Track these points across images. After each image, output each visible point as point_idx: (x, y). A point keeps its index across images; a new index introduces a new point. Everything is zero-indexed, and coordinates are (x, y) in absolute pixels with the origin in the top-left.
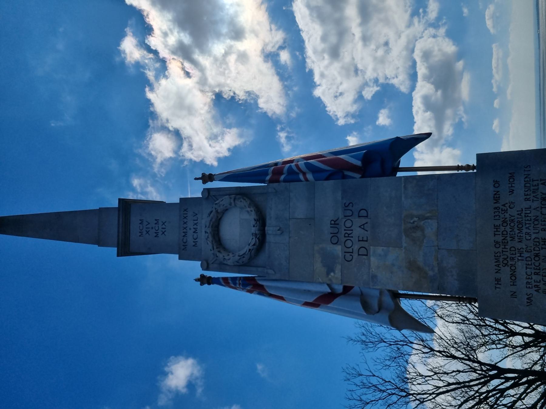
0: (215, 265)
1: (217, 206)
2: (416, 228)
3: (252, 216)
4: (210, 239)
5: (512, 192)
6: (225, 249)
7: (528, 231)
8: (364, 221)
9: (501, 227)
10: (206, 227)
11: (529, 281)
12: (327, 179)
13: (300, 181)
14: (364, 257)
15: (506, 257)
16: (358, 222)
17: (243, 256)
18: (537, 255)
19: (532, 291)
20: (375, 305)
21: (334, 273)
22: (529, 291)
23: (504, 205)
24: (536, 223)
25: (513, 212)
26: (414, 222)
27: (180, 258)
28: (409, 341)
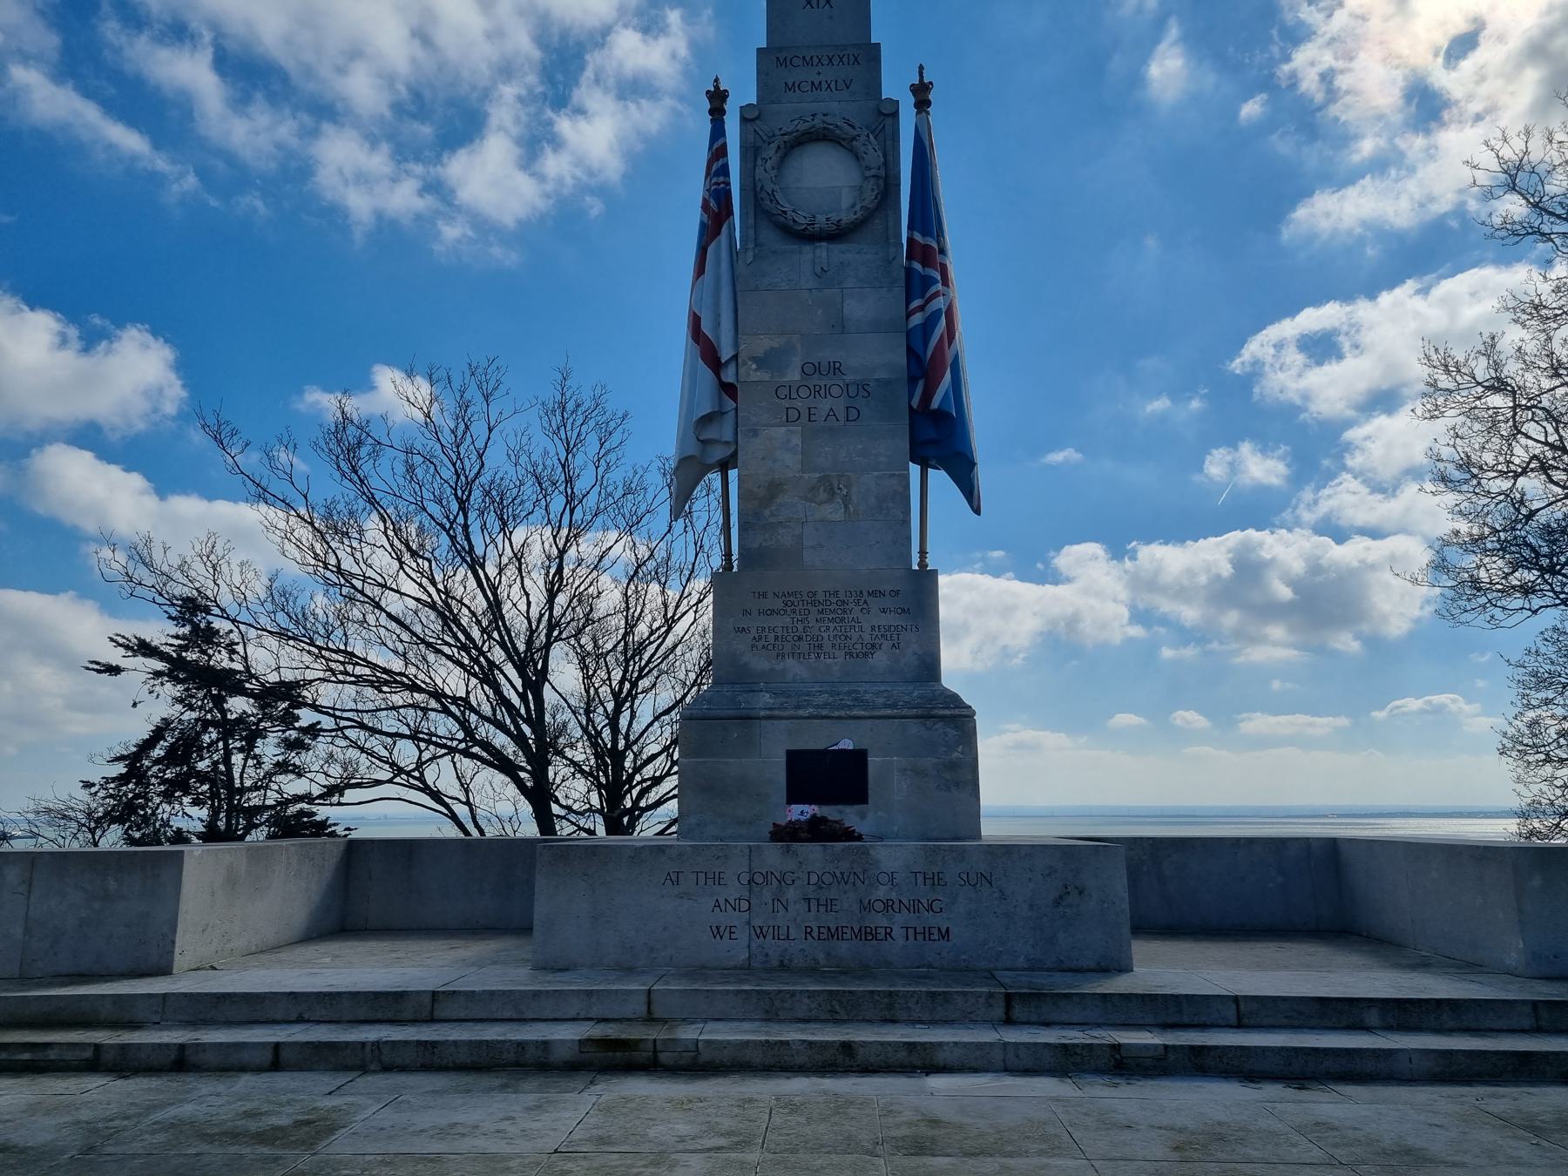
0: (751, 138)
1: (863, 138)
2: (832, 493)
3: (847, 217)
4: (803, 127)
5: (884, 611)
6: (783, 159)
7: (831, 629)
8: (842, 417)
9: (836, 599)
10: (824, 115)
11: (767, 630)
12: (910, 351)
13: (908, 303)
14: (785, 418)
15: (796, 604)
16: (840, 406)
17: (773, 199)
18: (800, 638)
19: (754, 633)
20: (709, 434)
21: (756, 370)
22: (754, 631)
23: (865, 602)
24: (843, 638)
25: (856, 613)
26: (839, 489)
27: (759, 50)
28: (575, 508)
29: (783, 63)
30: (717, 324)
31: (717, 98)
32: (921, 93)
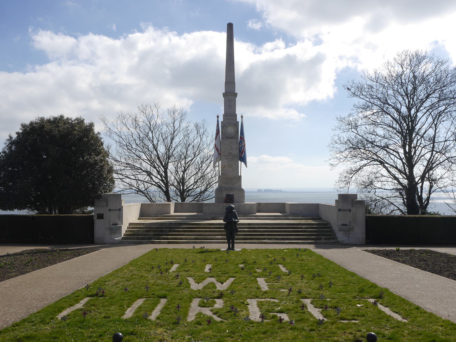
29: (226, 116)
30: (218, 146)
31: (218, 117)
32: (242, 117)
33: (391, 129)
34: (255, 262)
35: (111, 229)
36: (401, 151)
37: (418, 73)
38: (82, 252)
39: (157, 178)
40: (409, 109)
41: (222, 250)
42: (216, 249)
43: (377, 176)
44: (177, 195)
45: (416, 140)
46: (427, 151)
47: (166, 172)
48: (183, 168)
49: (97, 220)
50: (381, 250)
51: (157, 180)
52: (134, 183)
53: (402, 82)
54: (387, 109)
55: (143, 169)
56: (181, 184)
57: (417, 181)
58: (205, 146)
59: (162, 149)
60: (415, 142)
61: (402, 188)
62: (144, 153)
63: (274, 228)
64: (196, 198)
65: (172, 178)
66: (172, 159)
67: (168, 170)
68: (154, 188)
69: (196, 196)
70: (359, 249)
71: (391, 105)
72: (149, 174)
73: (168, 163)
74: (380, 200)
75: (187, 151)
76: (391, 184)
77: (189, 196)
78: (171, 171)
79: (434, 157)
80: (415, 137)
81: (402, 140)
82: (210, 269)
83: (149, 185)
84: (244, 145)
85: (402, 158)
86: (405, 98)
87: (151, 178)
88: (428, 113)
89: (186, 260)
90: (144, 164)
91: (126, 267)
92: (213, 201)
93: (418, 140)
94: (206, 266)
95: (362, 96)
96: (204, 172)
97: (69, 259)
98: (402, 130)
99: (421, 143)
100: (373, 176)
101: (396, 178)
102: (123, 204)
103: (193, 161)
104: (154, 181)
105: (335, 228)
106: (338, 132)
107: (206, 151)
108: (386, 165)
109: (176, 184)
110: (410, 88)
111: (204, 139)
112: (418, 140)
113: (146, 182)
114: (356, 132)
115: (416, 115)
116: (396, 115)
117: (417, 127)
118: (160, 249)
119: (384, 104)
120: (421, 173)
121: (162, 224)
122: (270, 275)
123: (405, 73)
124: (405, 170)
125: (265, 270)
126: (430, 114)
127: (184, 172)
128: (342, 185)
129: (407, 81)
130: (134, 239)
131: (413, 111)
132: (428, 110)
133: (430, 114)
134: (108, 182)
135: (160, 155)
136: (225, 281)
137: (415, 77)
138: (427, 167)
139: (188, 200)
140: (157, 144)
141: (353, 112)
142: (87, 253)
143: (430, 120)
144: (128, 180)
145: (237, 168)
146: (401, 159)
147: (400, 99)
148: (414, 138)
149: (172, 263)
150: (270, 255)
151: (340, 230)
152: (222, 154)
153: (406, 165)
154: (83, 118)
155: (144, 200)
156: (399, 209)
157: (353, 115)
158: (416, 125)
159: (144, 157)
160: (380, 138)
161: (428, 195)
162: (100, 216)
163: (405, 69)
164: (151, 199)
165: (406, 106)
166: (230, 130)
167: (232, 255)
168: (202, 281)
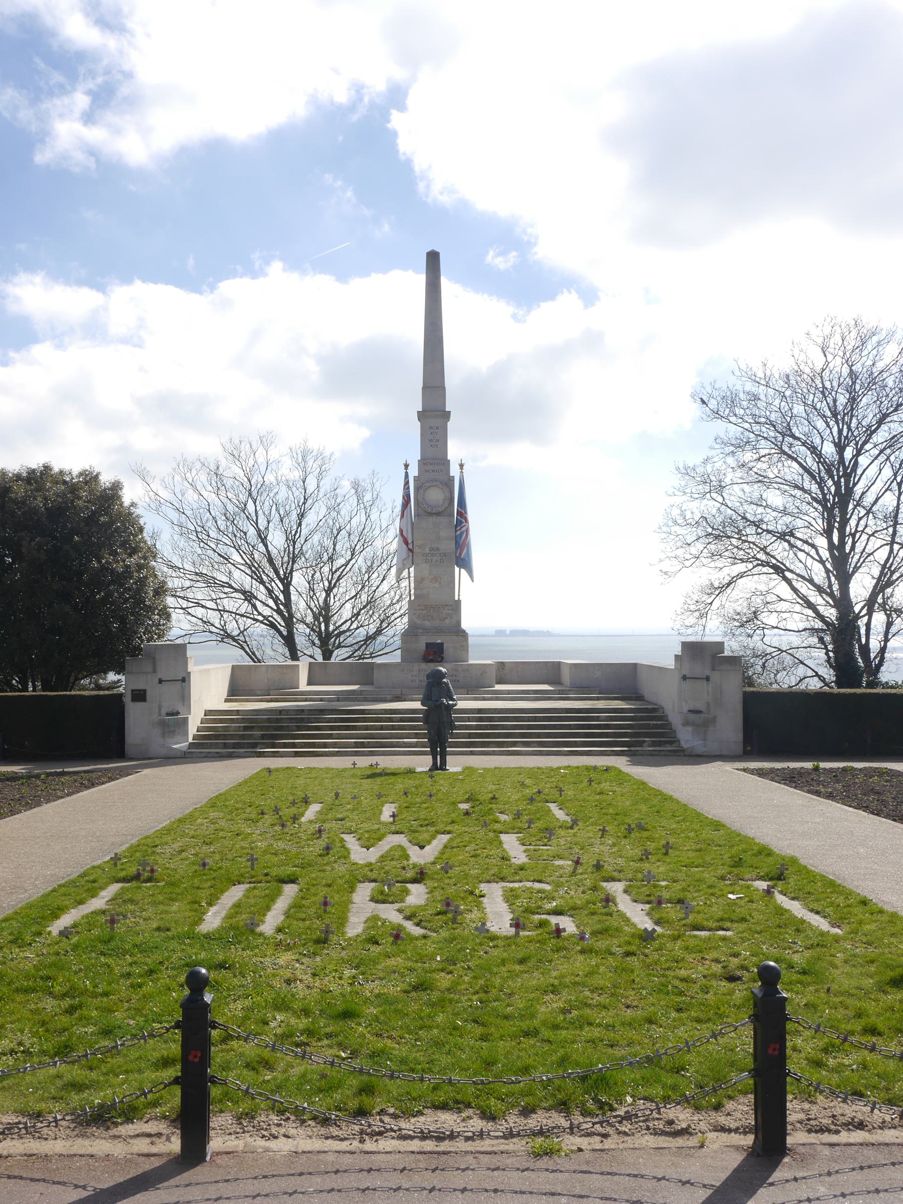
29: (425, 464)
30: (407, 532)
31: (406, 466)
32: (461, 466)
33: (798, 493)
34: (494, 798)
35: (163, 724)
36: (822, 542)
37: (859, 365)
38: (98, 778)
39: (267, 605)
40: (840, 448)
41: (418, 770)
42: (405, 769)
43: (769, 599)
44: (314, 644)
45: (855, 517)
46: (879, 543)
47: (286, 593)
48: (326, 584)
49: (132, 704)
50: (778, 769)
51: (267, 612)
52: (214, 617)
53: (824, 387)
54: (790, 448)
55: (234, 585)
56: (321, 619)
57: (857, 612)
58: (377, 532)
59: (277, 540)
60: (853, 522)
61: (825, 627)
62: (237, 550)
63: (535, 719)
64: (356, 651)
65: (300, 605)
66: (301, 562)
67: (292, 588)
68: (261, 629)
69: (356, 647)
70: (728, 767)
71: (798, 439)
72: (249, 596)
73: (292, 571)
74: (774, 654)
75: (335, 545)
76: (800, 619)
77: (339, 646)
78: (299, 590)
79: (894, 558)
80: (854, 509)
81: (823, 518)
82: (394, 816)
83: (249, 621)
84: (467, 531)
85: (824, 559)
86: (832, 423)
87: (254, 606)
88: (882, 458)
89: (337, 795)
90: (237, 574)
91: (202, 811)
92: (396, 658)
93: (860, 519)
94: (384, 809)
95: (733, 419)
96: (375, 591)
97: (68, 795)
98: (824, 495)
99: (866, 526)
100: (758, 601)
101: (810, 605)
102: (191, 667)
103: (349, 566)
104: (260, 614)
105: (675, 719)
106: (679, 499)
107: (378, 543)
108: (788, 574)
109: (310, 619)
110: (842, 400)
111: (374, 516)
112: (860, 519)
113: (242, 616)
114: (720, 499)
115: (856, 464)
116: (810, 462)
117: (858, 490)
118: (277, 770)
119: (783, 435)
120: (866, 594)
121: (280, 711)
122: (529, 827)
123: (831, 365)
124: (830, 586)
125: (518, 815)
126: (888, 458)
127: (328, 591)
128: (691, 620)
129: (835, 384)
130: (216, 746)
131: (849, 453)
132: (881, 452)
133: (888, 458)
134: (157, 617)
135: (274, 552)
136: (429, 843)
137: (852, 374)
138: (879, 579)
139: (339, 655)
140: (267, 528)
141: (714, 453)
142: (111, 779)
143: (888, 472)
144: (199, 612)
145: (451, 583)
146: (822, 562)
147: (820, 424)
148: (852, 514)
149: (306, 802)
150: (527, 781)
151: (686, 723)
152: (416, 550)
153: (833, 574)
154: (97, 470)
155: (237, 656)
156: (817, 675)
157: (715, 459)
158: (855, 484)
159: (236, 557)
160: (775, 514)
161: (882, 643)
162: (139, 696)
163: (830, 357)
164: (254, 653)
165: (834, 442)
166: (435, 496)
167: (442, 782)
168: (377, 843)
